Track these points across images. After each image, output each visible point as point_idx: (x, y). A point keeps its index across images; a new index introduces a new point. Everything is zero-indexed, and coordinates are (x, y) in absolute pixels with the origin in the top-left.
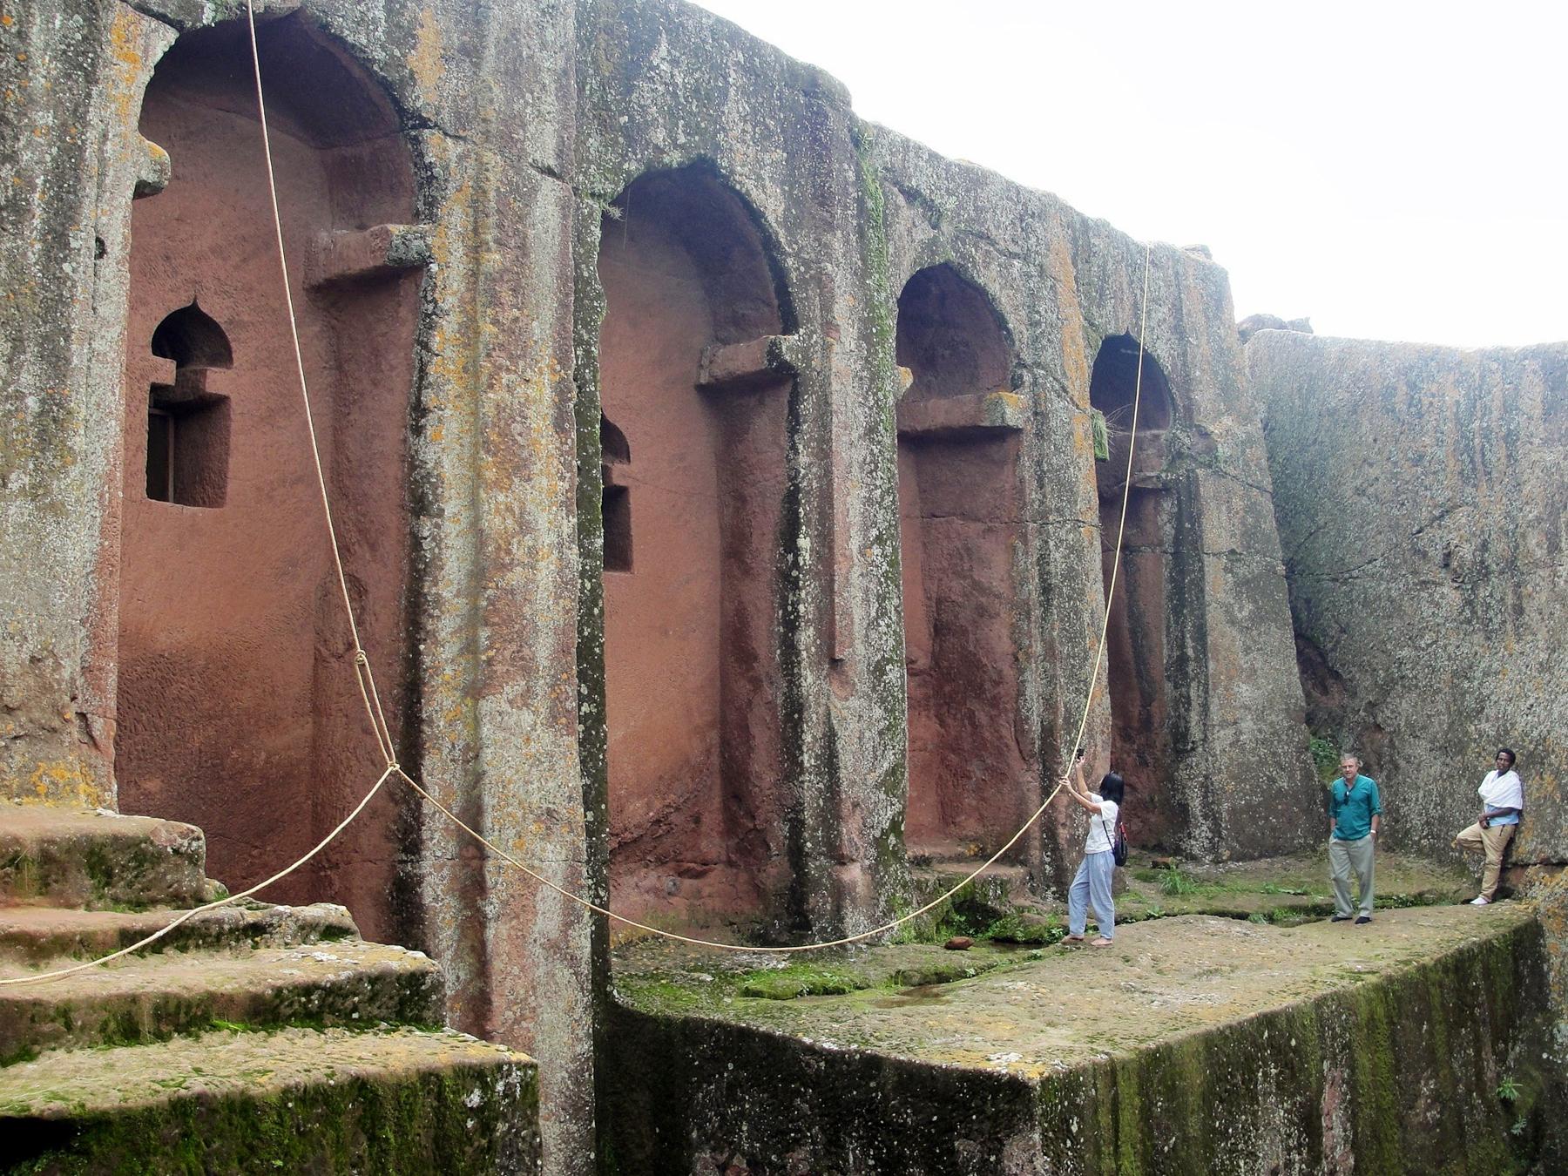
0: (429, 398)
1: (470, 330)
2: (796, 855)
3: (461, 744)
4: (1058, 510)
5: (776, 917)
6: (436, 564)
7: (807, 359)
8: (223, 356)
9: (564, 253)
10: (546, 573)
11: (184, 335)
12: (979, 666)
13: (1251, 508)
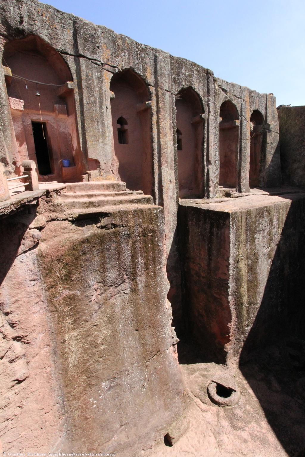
10: (169, 150)
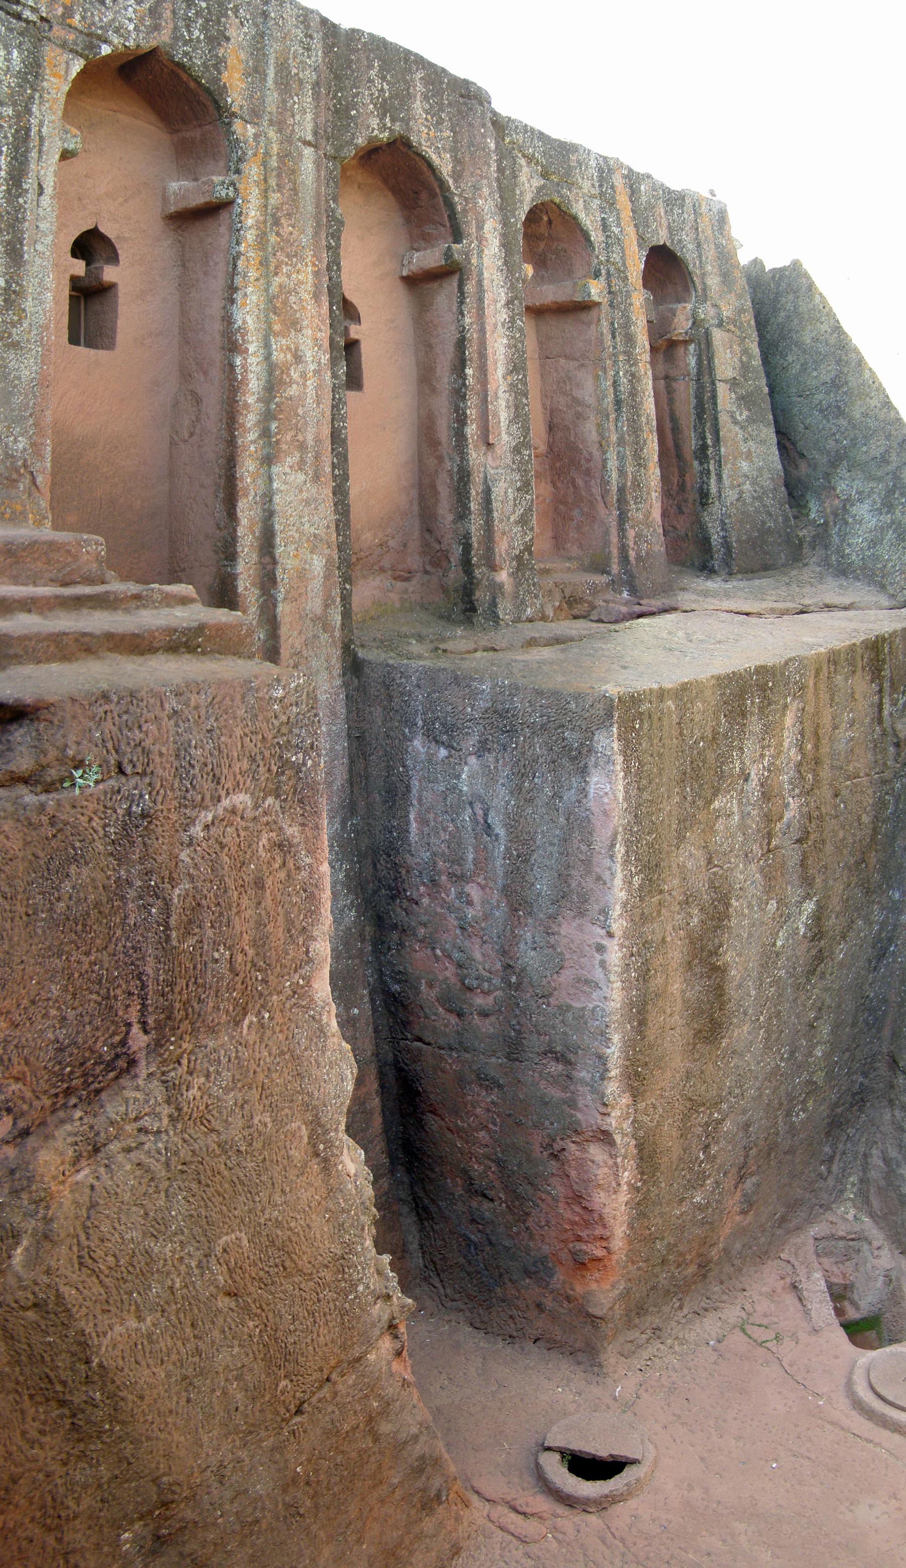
0: (238, 280)
1: (262, 239)
2: (467, 564)
3: (260, 492)
4: (625, 352)
5: (455, 604)
6: (245, 381)
7: (468, 258)
8: (113, 258)
9: (318, 194)
11: (90, 245)
12: (577, 450)
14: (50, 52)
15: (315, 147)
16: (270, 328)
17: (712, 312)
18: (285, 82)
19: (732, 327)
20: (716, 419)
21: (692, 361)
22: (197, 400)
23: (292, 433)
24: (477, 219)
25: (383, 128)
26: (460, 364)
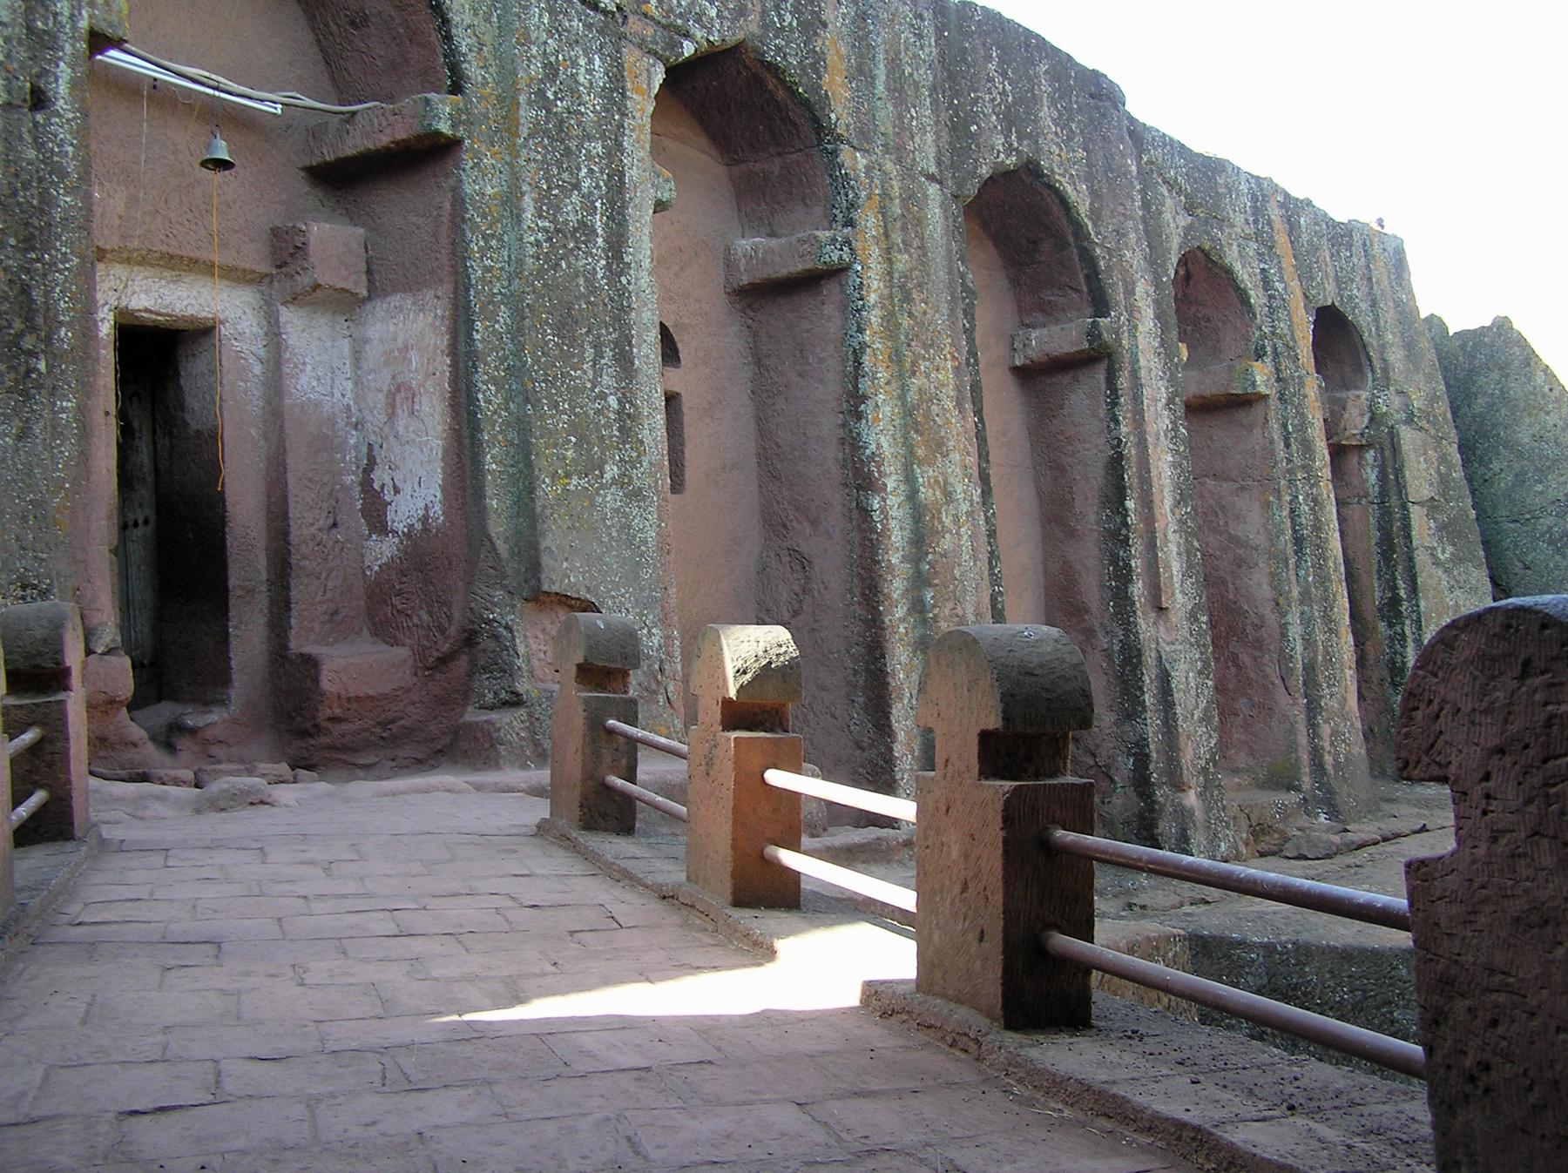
0: (865, 385)
1: (890, 322)
2: (1142, 783)
4: (1303, 467)
7: (1118, 340)
13: (1443, 459)
14: (630, 55)
15: (940, 183)
16: (912, 453)
17: (1397, 402)
18: (899, 88)
19: (1424, 424)
20: (1411, 559)
21: (1372, 476)
22: (802, 562)
23: (950, 605)
24: (1124, 280)
25: (1010, 149)
26: (1115, 494)
